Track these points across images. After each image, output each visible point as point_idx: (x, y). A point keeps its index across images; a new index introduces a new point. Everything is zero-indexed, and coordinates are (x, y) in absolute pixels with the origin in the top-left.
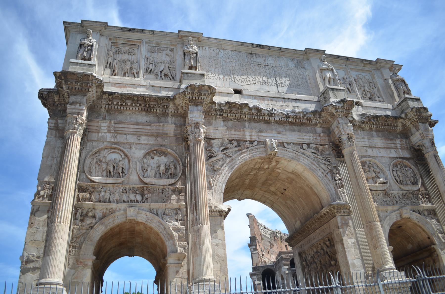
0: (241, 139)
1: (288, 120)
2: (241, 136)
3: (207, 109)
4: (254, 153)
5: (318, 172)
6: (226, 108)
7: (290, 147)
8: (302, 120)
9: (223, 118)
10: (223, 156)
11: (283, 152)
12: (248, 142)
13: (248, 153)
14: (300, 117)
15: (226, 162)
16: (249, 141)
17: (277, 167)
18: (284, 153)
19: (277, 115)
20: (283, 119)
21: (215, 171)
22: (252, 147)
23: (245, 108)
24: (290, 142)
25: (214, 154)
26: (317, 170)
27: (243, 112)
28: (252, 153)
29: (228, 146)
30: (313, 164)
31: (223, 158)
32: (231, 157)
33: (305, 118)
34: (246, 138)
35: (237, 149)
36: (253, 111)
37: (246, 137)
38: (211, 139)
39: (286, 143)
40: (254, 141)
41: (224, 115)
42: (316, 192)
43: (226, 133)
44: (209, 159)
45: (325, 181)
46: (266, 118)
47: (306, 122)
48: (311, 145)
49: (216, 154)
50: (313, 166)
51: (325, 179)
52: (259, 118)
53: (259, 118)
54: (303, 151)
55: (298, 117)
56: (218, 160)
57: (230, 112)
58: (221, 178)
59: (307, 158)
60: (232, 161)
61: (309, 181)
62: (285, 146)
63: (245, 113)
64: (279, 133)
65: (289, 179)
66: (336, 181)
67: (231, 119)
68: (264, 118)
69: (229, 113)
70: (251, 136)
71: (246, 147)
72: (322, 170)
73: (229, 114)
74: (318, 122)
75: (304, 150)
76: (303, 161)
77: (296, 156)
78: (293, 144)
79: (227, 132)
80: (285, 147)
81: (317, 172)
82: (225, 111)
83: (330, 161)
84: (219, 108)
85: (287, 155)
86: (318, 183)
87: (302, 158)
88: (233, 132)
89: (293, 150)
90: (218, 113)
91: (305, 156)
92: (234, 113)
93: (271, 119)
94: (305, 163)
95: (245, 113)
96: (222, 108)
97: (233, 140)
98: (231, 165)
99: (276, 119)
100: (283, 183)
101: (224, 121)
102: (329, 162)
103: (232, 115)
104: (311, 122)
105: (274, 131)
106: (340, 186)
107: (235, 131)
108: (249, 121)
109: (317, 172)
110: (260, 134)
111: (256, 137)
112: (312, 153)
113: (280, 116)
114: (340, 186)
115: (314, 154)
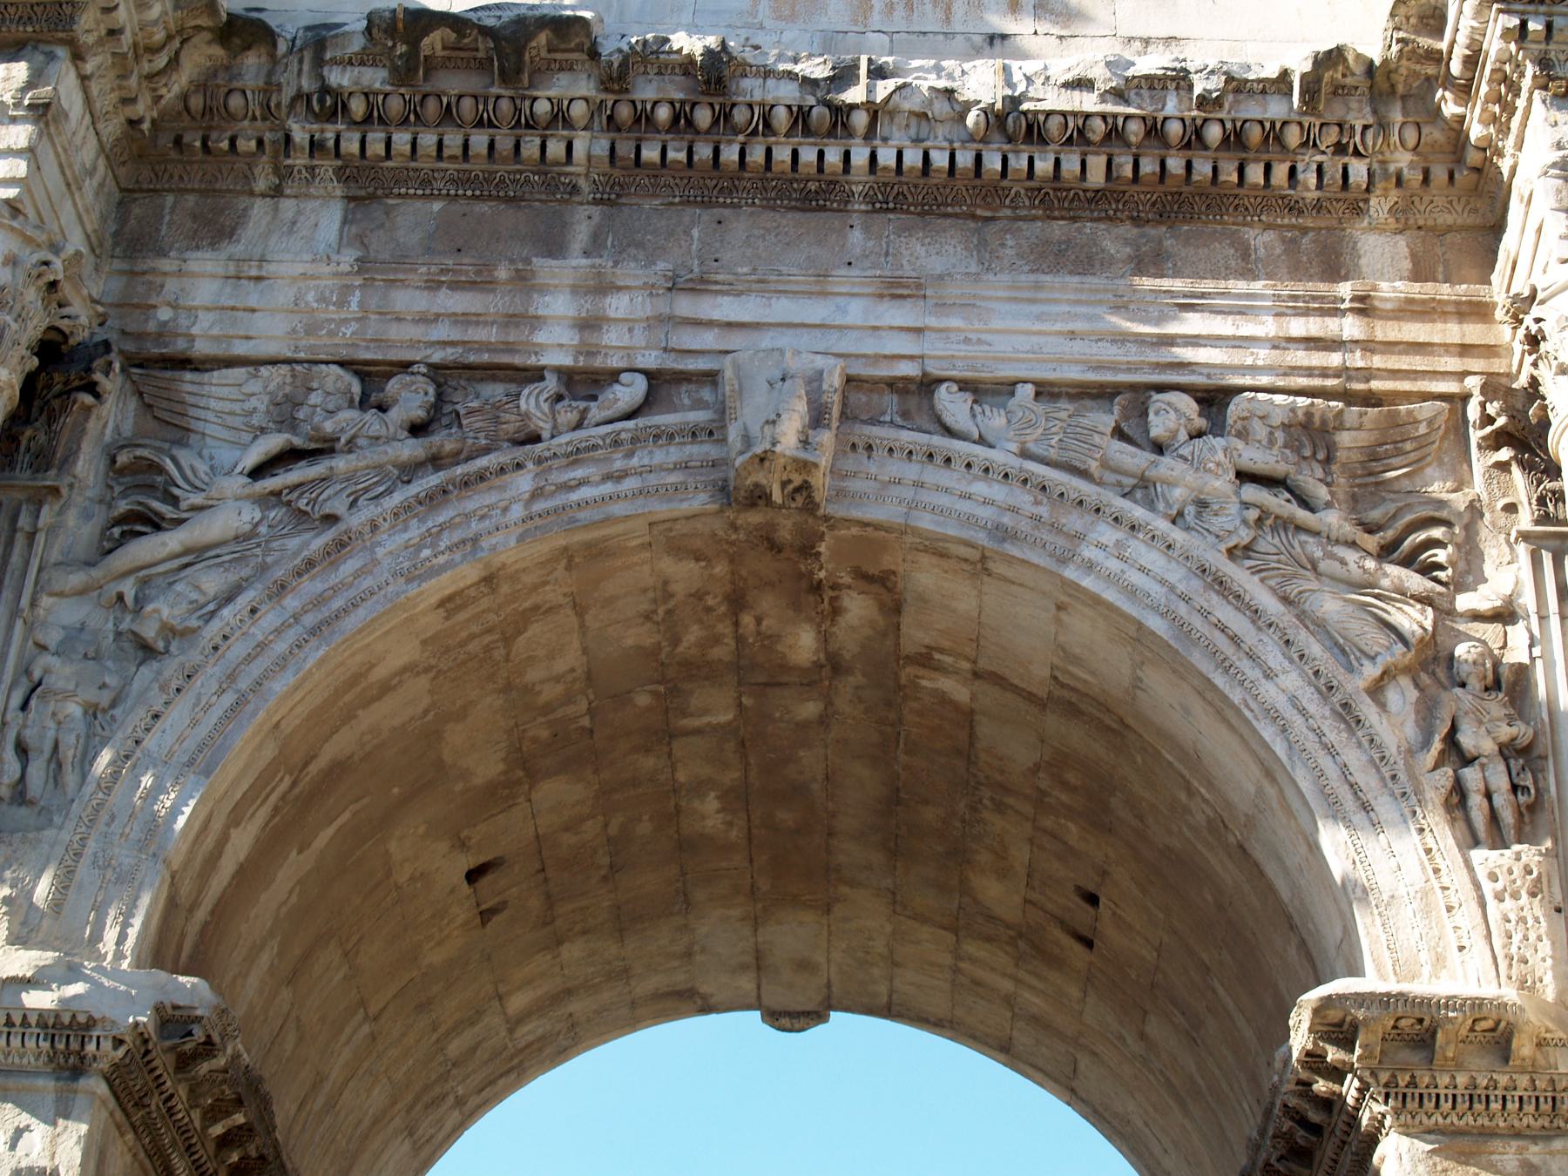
0: (486, 358)
1: (1019, 163)
2: (491, 334)
3: (185, 97)
4: (582, 483)
5: (1269, 675)
6: (375, 78)
7: (995, 421)
8: (1175, 165)
9: (343, 175)
10: (251, 513)
11: (911, 471)
12: (551, 384)
13: (524, 482)
14: (1154, 130)
15: (264, 568)
16: (569, 377)
17: (908, 648)
18: (919, 485)
19: (901, 120)
20: (965, 159)
21: (147, 651)
22: (579, 426)
23: (568, 67)
24: (1007, 372)
25: (174, 501)
26: (1251, 656)
27: (542, 107)
28: (567, 487)
29: (329, 427)
30: (1220, 585)
31: (251, 534)
32: (331, 519)
33: (1214, 133)
34: (538, 349)
35: (411, 449)
36: (646, 91)
37: (540, 337)
38: (184, 363)
39: (965, 385)
40: (614, 376)
41: (351, 145)
42: (1285, 893)
43: (342, 303)
44: (120, 543)
45: (1326, 762)
46: (782, 155)
47: (1229, 175)
48: (1236, 407)
49: (197, 499)
50: (1225, 613)
51: (1330, 750)
52: (704, 152)
53: (704, 152)
54: (1132, 458)
55: (1135, 130)
56: (196, 555)
57: (412, 117)
58: (178, 715)
59: (1162, 525)
60: (334, 565)
61: (1210, 784)
62: (949, 420)
63: (560, 117)
64: (896, 290)
65: (1071, 777)
66: (1468, 761)
67: (426, 182)
68: (756, 155)
69: (404, 122)
70: (589, 324)
71: (511, 425)
72: (1315, 649)
73: (402, 139)
74: (1358, 171)
75: (1159, 448)
76: (1114, 565)
77: (1043, 511)
78: (1046, 391)
79: (355, 300)
80: (949, 432)
81: (1252, 673)
82: (358, 107)
83: (1441, 556)
84: (307, 84)
85: (944, 500)
86: (1271, 791)
87: (1107, 534)
88: (409, 300)
89: (1025, 454)
90: (300, 135)
91: (1138, 513)
92: (448, 115)
93: (833, 157)
94: (1135, 578)
95: (560, 117)
96: (338, 78)
97: (405, 366)
98: (319, 601)
99: (887, 157)
100: (1048, 822)
101: (354, 201)
102: (1428, 570)
103: (428, 140)
104: (1280, 172)
105: (843, 279)
106: (1508, 817)
107: (433, 285)
108: (611, 195)
109: (1252, 673)
110: (685, 306)
111: (639, 338)
112: (1244, 476)
113: (941, 131)
114: (1508, 817)
115: (1251, 492)
